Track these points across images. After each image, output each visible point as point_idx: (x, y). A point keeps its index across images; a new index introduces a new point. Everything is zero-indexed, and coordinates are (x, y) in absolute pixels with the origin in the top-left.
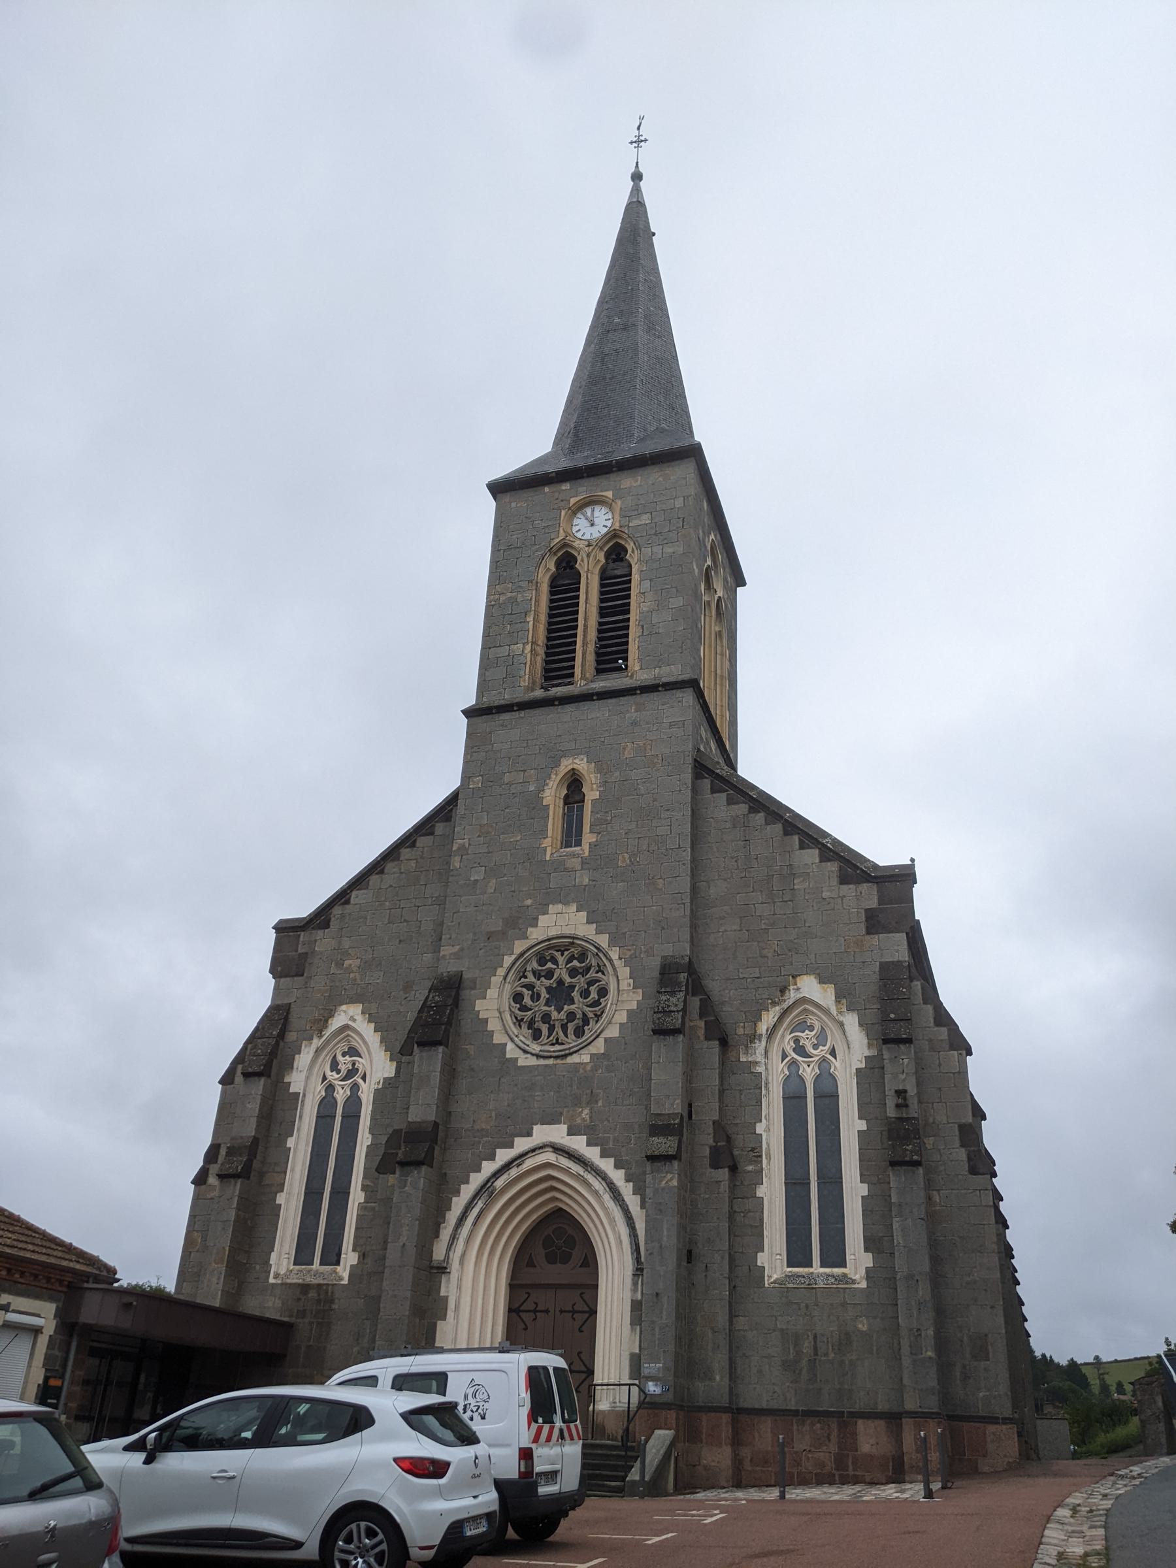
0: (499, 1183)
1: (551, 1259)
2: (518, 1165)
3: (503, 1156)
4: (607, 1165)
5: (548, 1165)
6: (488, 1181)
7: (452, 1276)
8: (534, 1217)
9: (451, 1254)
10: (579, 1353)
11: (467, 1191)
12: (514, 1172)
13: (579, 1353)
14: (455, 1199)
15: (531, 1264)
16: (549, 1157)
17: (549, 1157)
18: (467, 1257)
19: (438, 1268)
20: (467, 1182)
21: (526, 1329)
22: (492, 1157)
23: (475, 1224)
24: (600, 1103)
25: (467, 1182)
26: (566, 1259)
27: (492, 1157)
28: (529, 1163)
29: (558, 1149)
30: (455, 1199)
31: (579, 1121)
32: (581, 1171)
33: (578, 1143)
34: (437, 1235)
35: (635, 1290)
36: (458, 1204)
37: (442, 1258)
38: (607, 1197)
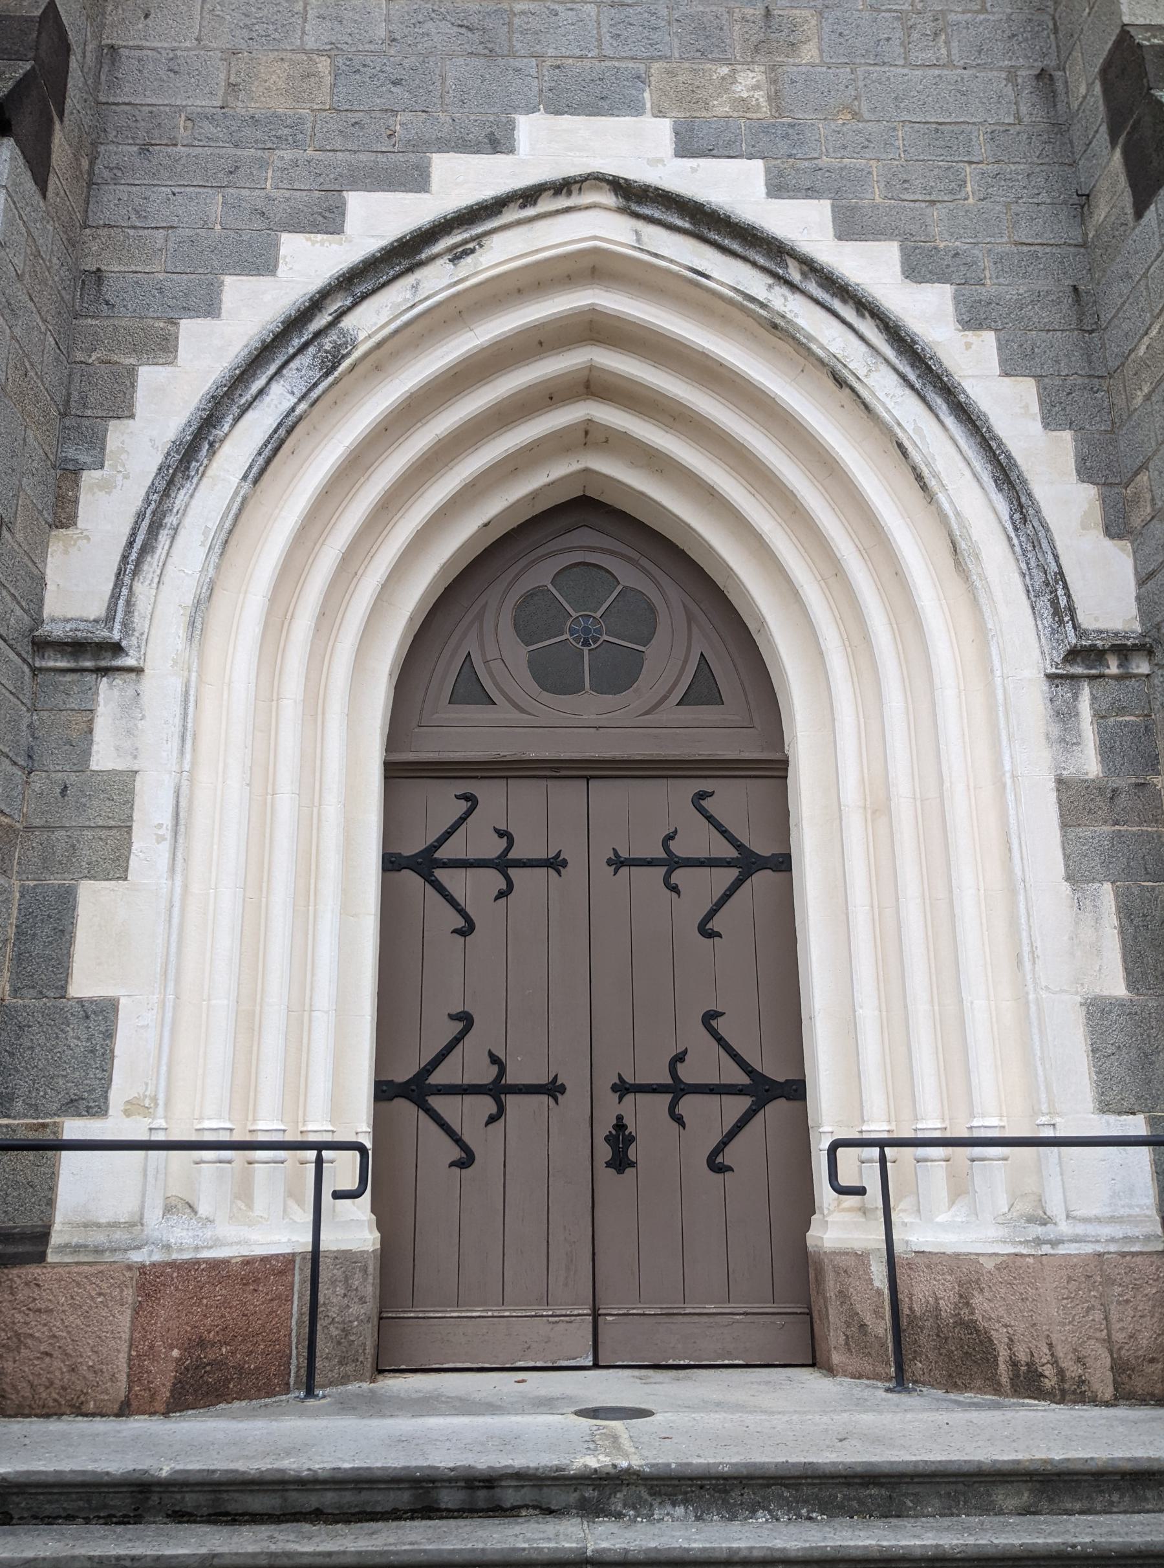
0: (370, 320)
1: (555, 677)
2: (458, 255)
3: (376, 218)
4: (872, 267)
5: (594, 267)
6: (316, 304)
7: (148, 682)
8: (493, 507)
9: (143, 590)
10: (709, 1018)
11: (208, 349)
12: (436, 280)
13: (709, 1018)
14: (148, 376)
15: (470, 690)
16: (603, 227)
17: (603, 227)
18: (222, 601)
19: (77, 647)
20: (210, 307)
21: (467, 929)
22: (327, 220)
23: (260, 472)
24: (809, 53)
25: (210, 307)
26: (618, 675)
27: (327, 220)
28: (505, 250)
29: (634, 197)
30: (148, 376)
31: (721, 108)
32: (755, 284)
33: (734, 185)
34: (62, 513)
35: (1067, 740)
36: (166, 398)
37: (96, 608)
38: (886, 388)
